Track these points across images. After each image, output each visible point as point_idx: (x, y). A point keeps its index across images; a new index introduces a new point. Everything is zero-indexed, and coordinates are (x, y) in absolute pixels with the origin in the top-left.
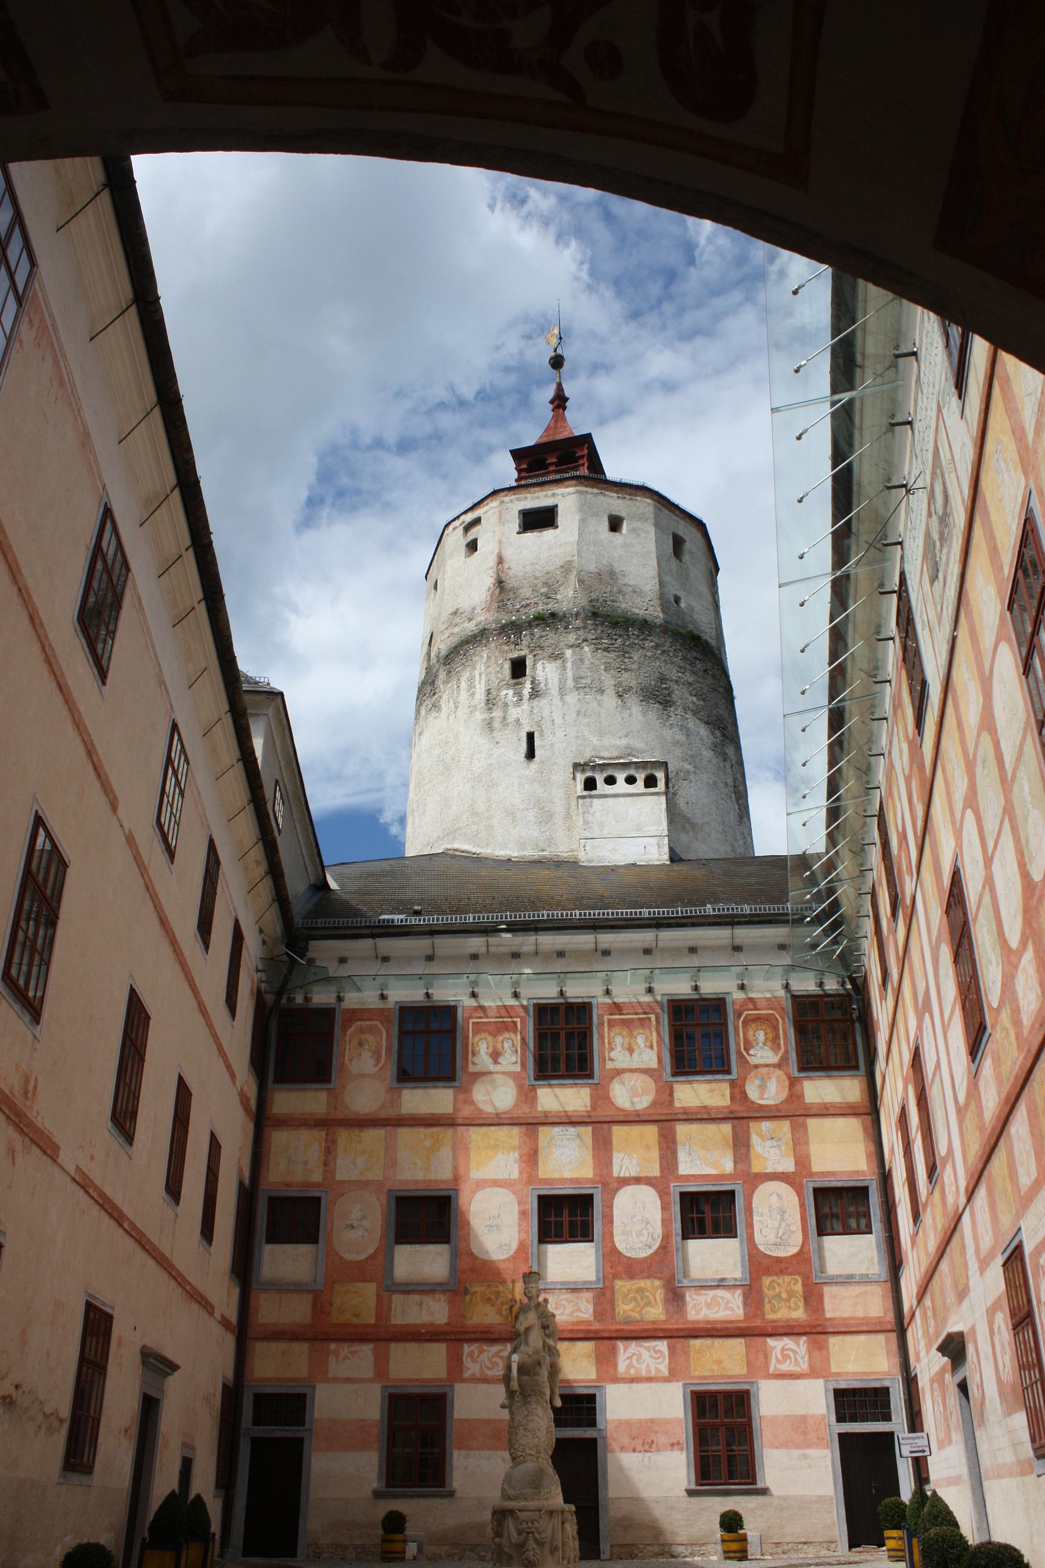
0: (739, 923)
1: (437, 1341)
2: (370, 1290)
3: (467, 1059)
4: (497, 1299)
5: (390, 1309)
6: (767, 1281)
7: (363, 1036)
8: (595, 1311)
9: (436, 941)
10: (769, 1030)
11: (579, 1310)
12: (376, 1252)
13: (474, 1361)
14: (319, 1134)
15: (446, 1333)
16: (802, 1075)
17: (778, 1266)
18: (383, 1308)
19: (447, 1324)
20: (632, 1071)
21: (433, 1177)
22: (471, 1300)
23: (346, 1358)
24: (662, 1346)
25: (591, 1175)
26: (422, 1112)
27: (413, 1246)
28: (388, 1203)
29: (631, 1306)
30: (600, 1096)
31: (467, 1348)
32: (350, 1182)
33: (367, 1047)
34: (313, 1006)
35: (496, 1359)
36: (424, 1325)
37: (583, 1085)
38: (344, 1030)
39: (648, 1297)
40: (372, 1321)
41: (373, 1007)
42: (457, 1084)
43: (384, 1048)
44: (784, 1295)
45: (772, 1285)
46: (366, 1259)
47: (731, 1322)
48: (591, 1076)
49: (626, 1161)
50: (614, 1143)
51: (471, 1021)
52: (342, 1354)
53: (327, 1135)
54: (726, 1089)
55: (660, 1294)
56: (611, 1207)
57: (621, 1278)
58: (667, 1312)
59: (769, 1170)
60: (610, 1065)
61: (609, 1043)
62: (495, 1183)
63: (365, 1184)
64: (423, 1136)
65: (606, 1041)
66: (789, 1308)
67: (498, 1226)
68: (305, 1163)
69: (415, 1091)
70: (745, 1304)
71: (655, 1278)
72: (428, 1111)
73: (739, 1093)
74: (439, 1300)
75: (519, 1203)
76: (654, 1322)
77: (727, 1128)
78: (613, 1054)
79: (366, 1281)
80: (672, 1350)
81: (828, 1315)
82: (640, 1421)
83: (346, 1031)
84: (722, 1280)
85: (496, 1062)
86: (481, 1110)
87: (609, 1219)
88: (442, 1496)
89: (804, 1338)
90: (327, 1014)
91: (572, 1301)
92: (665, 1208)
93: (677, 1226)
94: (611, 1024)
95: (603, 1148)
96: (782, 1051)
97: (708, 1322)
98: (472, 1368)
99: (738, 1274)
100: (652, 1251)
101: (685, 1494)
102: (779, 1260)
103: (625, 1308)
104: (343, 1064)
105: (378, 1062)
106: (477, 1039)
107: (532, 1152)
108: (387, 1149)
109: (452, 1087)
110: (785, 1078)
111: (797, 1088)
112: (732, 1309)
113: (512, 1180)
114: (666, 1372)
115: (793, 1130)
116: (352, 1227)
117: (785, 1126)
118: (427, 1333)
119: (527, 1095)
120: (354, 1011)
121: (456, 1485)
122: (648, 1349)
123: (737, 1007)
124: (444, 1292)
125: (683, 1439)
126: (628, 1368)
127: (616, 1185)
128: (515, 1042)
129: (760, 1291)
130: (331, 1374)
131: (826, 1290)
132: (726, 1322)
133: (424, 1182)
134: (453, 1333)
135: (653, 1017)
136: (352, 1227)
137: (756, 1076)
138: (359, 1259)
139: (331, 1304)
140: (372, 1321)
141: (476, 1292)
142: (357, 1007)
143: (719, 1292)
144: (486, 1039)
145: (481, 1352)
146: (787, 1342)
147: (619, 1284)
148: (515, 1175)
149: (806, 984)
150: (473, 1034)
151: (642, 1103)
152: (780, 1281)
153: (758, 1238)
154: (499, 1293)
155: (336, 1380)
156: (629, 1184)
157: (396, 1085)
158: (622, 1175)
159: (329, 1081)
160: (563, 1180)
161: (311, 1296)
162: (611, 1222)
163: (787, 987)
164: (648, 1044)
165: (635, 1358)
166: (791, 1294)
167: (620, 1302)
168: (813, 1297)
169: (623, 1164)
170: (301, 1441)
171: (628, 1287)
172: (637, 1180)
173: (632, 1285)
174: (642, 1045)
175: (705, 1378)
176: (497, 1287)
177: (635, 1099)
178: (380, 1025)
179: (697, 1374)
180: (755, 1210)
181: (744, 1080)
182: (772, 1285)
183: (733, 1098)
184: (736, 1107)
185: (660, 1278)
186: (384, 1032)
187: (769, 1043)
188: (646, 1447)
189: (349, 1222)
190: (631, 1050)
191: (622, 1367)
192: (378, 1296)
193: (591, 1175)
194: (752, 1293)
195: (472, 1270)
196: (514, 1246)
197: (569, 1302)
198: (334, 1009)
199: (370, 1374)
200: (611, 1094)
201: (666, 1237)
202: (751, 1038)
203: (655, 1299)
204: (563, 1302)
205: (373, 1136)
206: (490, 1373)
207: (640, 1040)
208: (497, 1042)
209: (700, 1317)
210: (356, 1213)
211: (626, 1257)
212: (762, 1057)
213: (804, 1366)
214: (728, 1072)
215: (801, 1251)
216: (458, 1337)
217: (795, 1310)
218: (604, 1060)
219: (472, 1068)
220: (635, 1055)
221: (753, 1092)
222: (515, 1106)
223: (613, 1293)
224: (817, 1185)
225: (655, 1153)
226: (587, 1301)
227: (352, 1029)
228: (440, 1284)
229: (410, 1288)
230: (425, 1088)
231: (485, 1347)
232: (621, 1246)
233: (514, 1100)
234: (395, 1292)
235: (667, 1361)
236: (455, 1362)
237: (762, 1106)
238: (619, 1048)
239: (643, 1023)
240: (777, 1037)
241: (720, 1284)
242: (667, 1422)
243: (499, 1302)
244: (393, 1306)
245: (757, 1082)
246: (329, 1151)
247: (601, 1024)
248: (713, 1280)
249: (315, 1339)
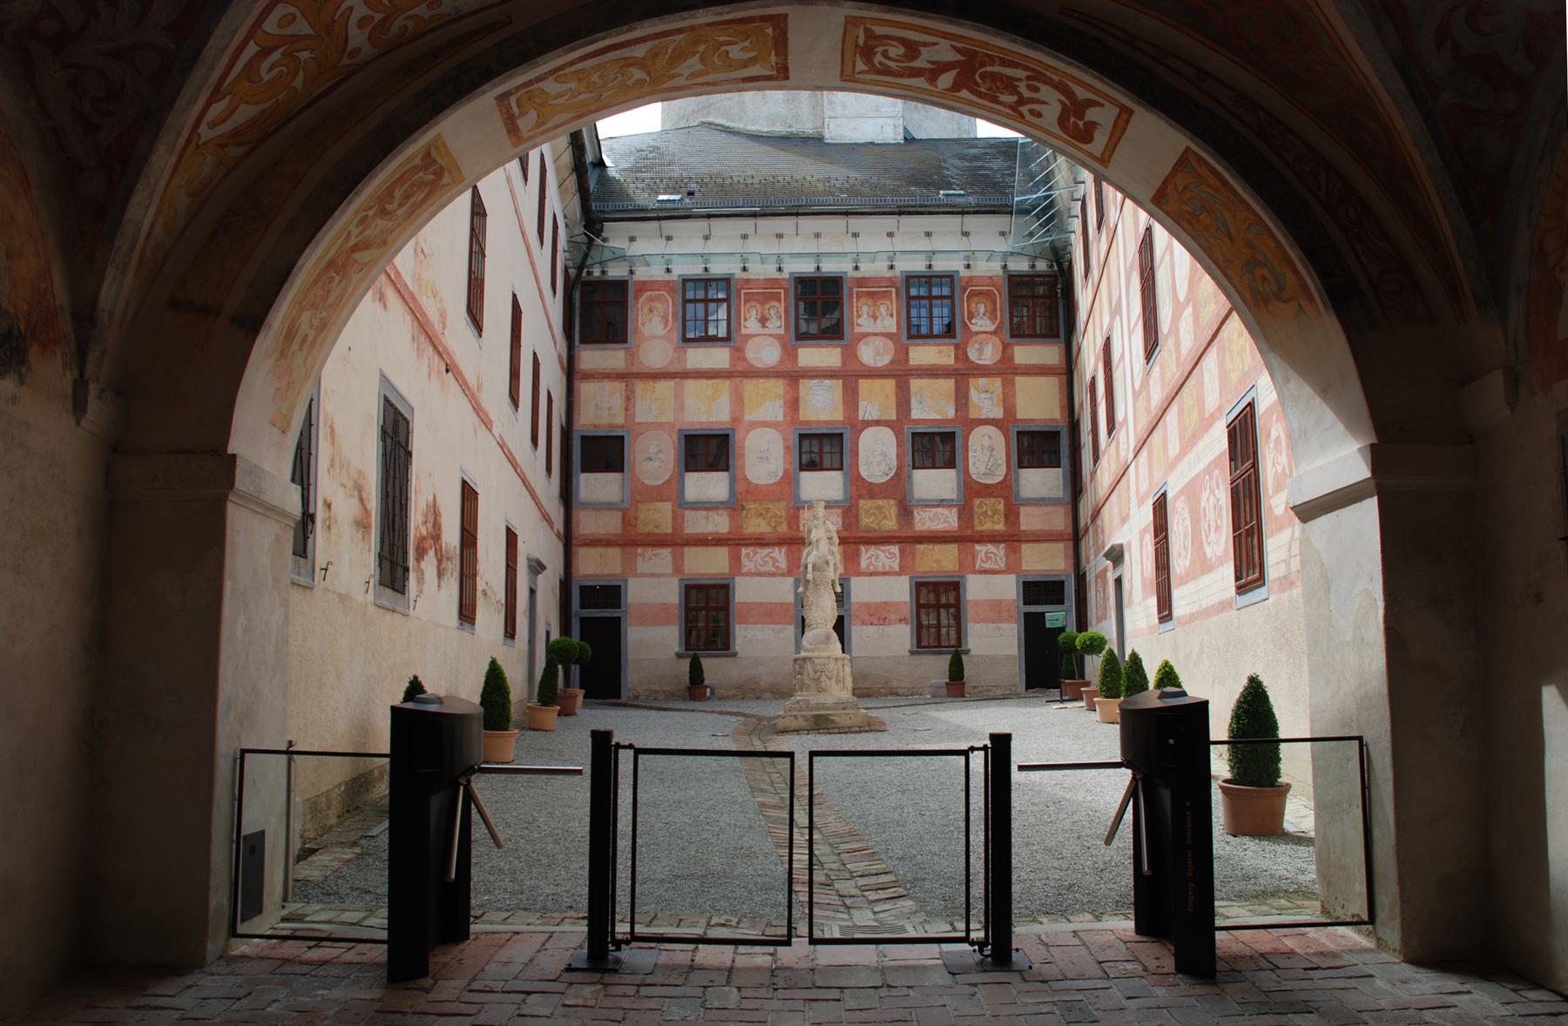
0: (968, 213)
1: (721, 545)
2: (667, 507)
5: (683, 522)
6: (977, 501)
7: (653, 304)
9: (712, 223)
10: (988, 304)
12: (670, 478)
13: (750, 560)
14: (619, 386)
16: (1013, 341)
17: (987, 491)
18: (677, 521)
20: (875, 334)
24: (895, 549)
25: (841, 418)
26: (704, 367)
28: (679, 442)
30: (850, 354)
31: (744, 551)
33: (656, 312)
35: (768, 559)
36: (710, 534)
37: (836, 347)
38: (636, 298)
40: (670, 531)
42: (732, 344)
44: (989, 513)
45: (980, 505)
47: (948, 532)
48: (842, 338)
49: (870, 407)
50: (860, 393)
51: (743, 291)
52: (647, 556)
54: (951, 350)
55: (894, 511)
56: (857, 444)
57: (864, 498)
58: (899, 523)
59: (983, 417)
60: (857, 330)
62: (765, 424)
63: (659, 426)
66: (993, 522)
68: (610, 409)
69: (698, 350)
70: (959, 518)
71: (891, 498)
73: (961, 354)
75: (784, 440)
76: (889, 532)
77: (949, 384)
78: (860, 321)
80: (902, 552)
81: (1023, 528)
82: (877, 603)
84: (942, 500)
85: (764, 326)
86: (752, 366)
87: (855, 454)
88: (727, 656)
89: (1003, 545)
90: (621, 286)
92: (899, 444)
93: (909, 459)
94: (859, 295)
95: (851, 398)
96: (998, 321)
97: (931, 532)
98: (748, 565)
99: (954, 496)
101: (908, 654)
102: (987, 486)
103: (866, 521)
105: (666, 325)
106: (748, 306)
108: (676, 397)
110: (999, 342)
111: (1009, 351)
112: (949, 522)
114: (897, 568)
115: (1004, 385)
116: (650, 459)
117: (997, 383)
118: (713, 540)
119: (790, 353)
120: (644, 282)
121: (737, 648)
122: (884, 551)
123: (963, 283)
124: (724, 508)
125: (908, 615)
126: (868, 565)
129: (971, 510)
131: (1022, 509)
132: (944, 532)
134: (735, 539)
135: (894, 290)
136: (650, 459)
137: (976, 342)
140: (670, 531)
142: (646, 279)
143: (940, 510)
145: (755, 553)
146: (990, 547)
147: (862, 503)
148: (781, 418)
149: (1020, 266)
150: (746, 302)
151: (883, 361)
152: (987, 502)
153: (972, 470)
154: (769, 509)
157: (682, 344)
159: (625, 341)
160: (819, 422)
162: (857, 455)
163: (1005, 267)
165: (873, 558)
166: (995, 512)
168: (1012, 514)
169: (867, 410)
172: (878, 423)
175: (926, 572)
177: (878, 358)
179: (921, 570)
180: (970, 448)
181: (966, 344)
182: (980, 505)
183: (956, 358)
184: (959, 366)
187: (988, 315)
188: (881, 622)
190: (875, 318)
191: (864, 564)
192: (673, 512)
193: (841, 418)
194: (965, 512)
196: (780, 474)
198: (627, 281)
200: (858, 353)
201: (900, 468)
202: (973, 310)
205: (664, 387)
206: (763, 569)
207: (883, 309)
209: (925, 528)
210: (653, 449)
212: (981, 326)
213: (1002, 565)
214: (954, 337)
215: (1004, 479)
217: (998, 523)
218: (853, 325)
219: (744, 331)
220: (879, 321)
221: (973, 354)
222: (781, 362)
223: (857, 509)
224: (1020, 429)
225: (893, 401)
227: (643, 298)
228: (722, 503)
229: (698, 506)
231: (758, 550)
232: (864, 473)
233: (779, 358)
234: (687, 509)
235: (898, 560)
236: (736, 561)
237: (979, 365)
238: (865, 316)
239: (887, 295)
240: (995, 309)
241: (941, 503)
242: (896, 604)
243: (769, 515)
245: (977, 346)
246: (629, 398)
247: (851, 295)
248: (936, 501)
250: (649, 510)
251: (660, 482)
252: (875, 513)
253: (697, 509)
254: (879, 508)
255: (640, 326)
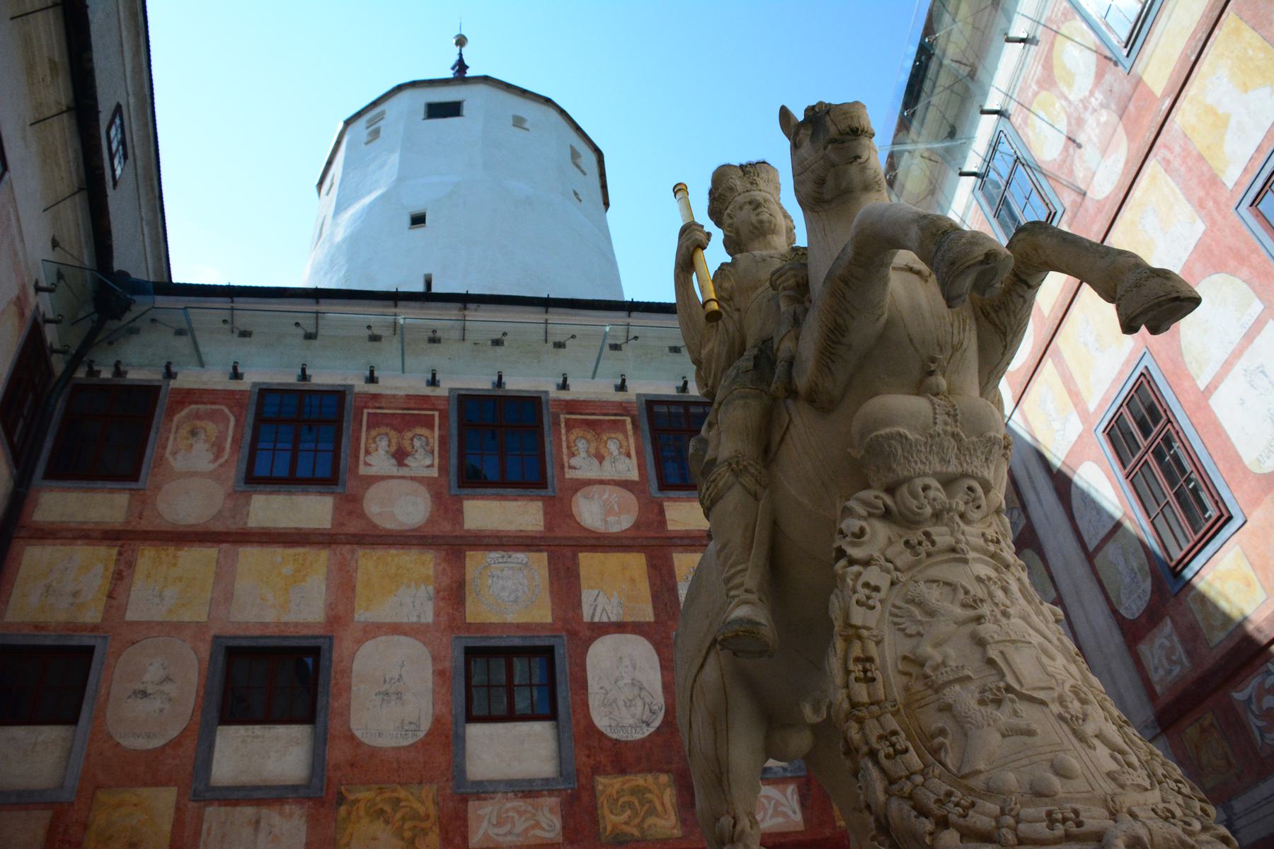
2: (164, 799)
3: (357, 458)
4: (395, 811)
5: (197, 833)
7: (198, 423)
8: (564, 828)
11: (537, 825)
12: (183, 735)
21: (292, 617)
22: (349, 813)
27: (250, 727)
28: (212, 655)
29: (624, 817)
30: (559, 509)
32: (149, 625)
34: (126, 383)
37: (533, 499)
38: (171, 413)
39: (650, 802)
41: (219, 387)
43: (229, 440)
46: (163, 748)
49: (602, 600)
51: (366, 411)
53: (120, 554)
55: (669, 796)
57: (606, 773)
61: (569, 447)
62: (396, 629)
63: (176, 628)
64: (279, 559)
65: (564, 445)
67: (399, 694)
72: (292, 525)
74: (291, 815)
78: (574, 461)
79: (156, 783)
83: (173, 416)
91: (525, 812)
100: (651, 730)
104: (162, 457)
105: (217, 457)
107: (455, 586)
109: (332, 493)
113: (422, 625)
116: (144, 694)
119: (446, 506)
124: (299, 801)
127: (588, 633)
128: (431, 440)
133: (277, 624)
136: (144, 694)
138: (150, 747)
139: (85, 826)
141: (357, 801)
144: (387, 434)
147: (602, 782)
148: (429, 617)
151: (622, 523)
154: (398, 800)
156: (607, 633)
157: (243, 487)
158: (596, 620)
160: (504, 626)
164: (623, 450)
167: (606, 811)
171: (617, 786)
172: (620, 627)
173: (624, 783)
174: (616, 453)
176: (394, 791)
177: (611, 519)
178: (226, 410)
185: (667, 772)
186: (232, 419)
189: (141, 687)
190: (600, 458)
192: (179, 809)
193: (549, 620)
195: (352, 765)
196: (426, 726)
197: (520, 813)
200: (574, 510)
203: (663, 804)
204: (511, 814)
207: (613, 446)
208: (403, 439)
210: (153, 673)
211: (611, 740)
219: (363, 470)
220: (607, 463)
223: (593, 795)
226: (551, 811)
227: (183, 413)
228: (295, 788)
230: (290, 493)
233: (428, 514)
234: (210, 802)
238: (583, 454)
243: (399, 815)
244: (205, 827)
246: (120, 577)
252: (630, 805)
254: (637, 791)
255: (168, 454)
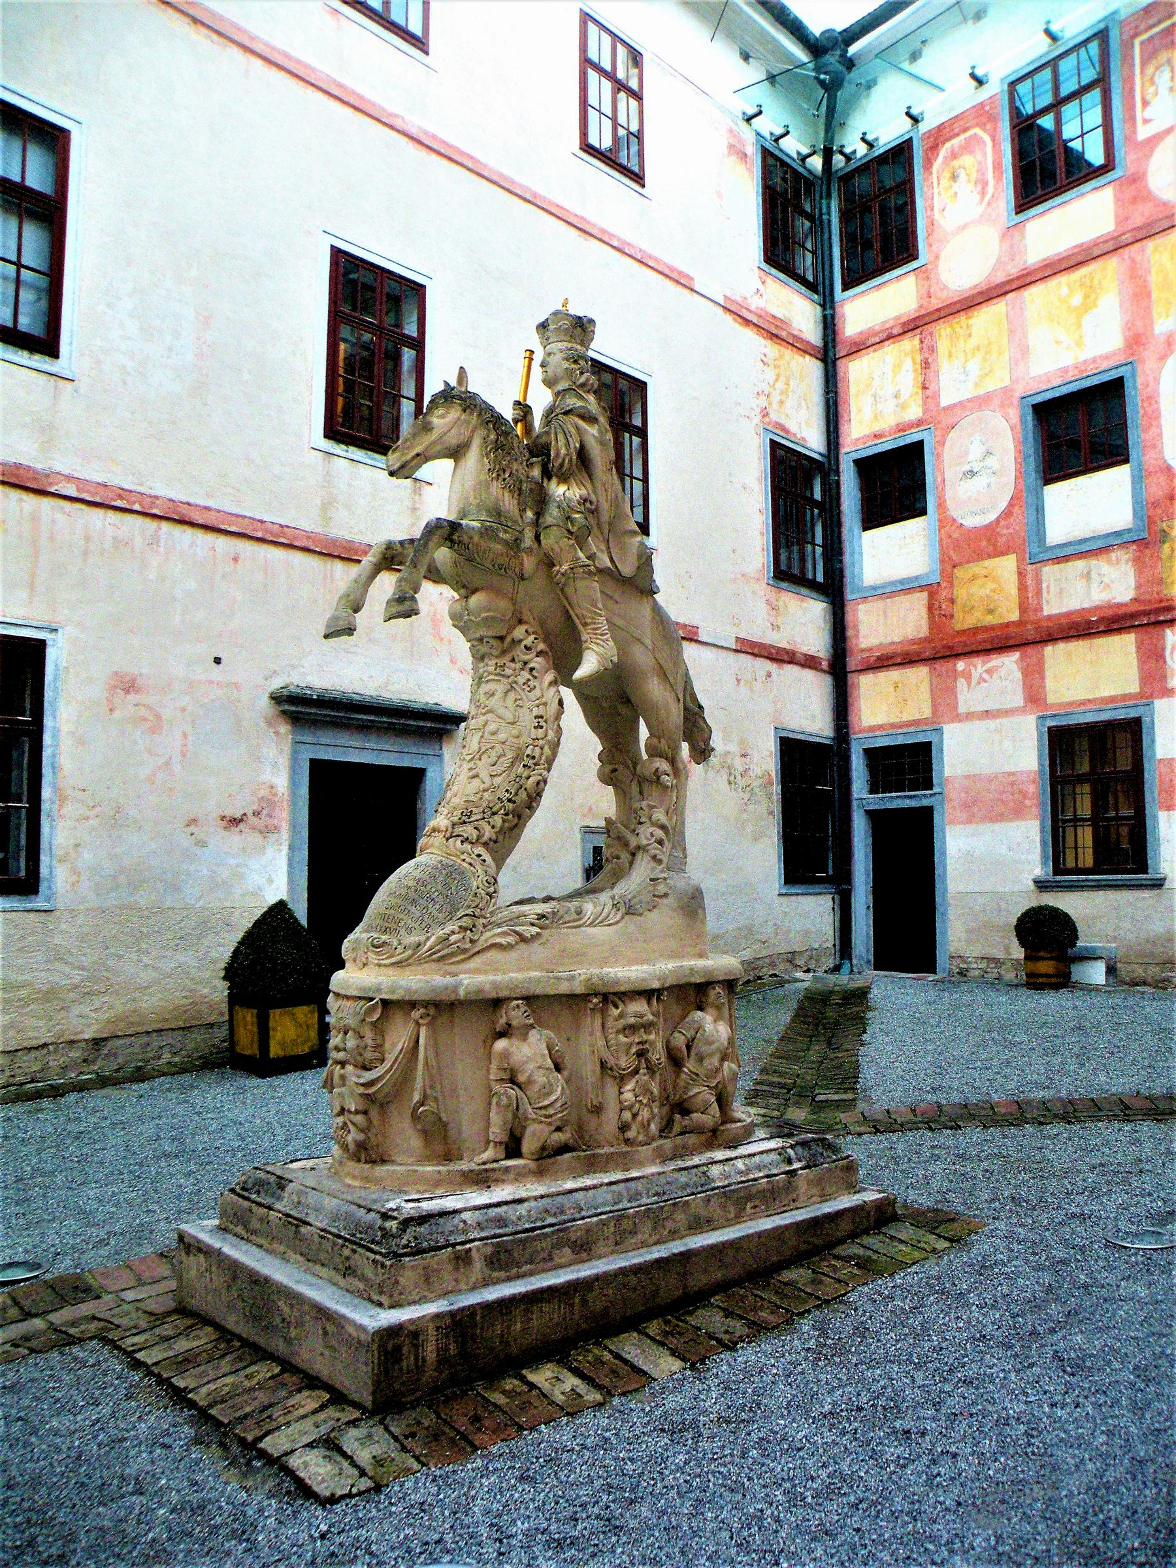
1: (1119, 631)
12: (1011, 505)
15: (1133, 615)
19: (1135, 600)
23: (982, 680)
46: (998, 521)
74: (1118, 561)
124: (1124, 545)
130: (962, 709)
138: (987, 521)
139: (952, 601)
140: (1015, 616)
155: (970, 716)
161: (925, 595)
170: (928, 812)
192: (1021, 574)
199: (1018, 700)
216: (1153, 619)
228: (1118, 534)
244: (1044, 586)
249: (935, 659)
250: (974, 578)
251: (992, 517)
253: (1066, 558)
